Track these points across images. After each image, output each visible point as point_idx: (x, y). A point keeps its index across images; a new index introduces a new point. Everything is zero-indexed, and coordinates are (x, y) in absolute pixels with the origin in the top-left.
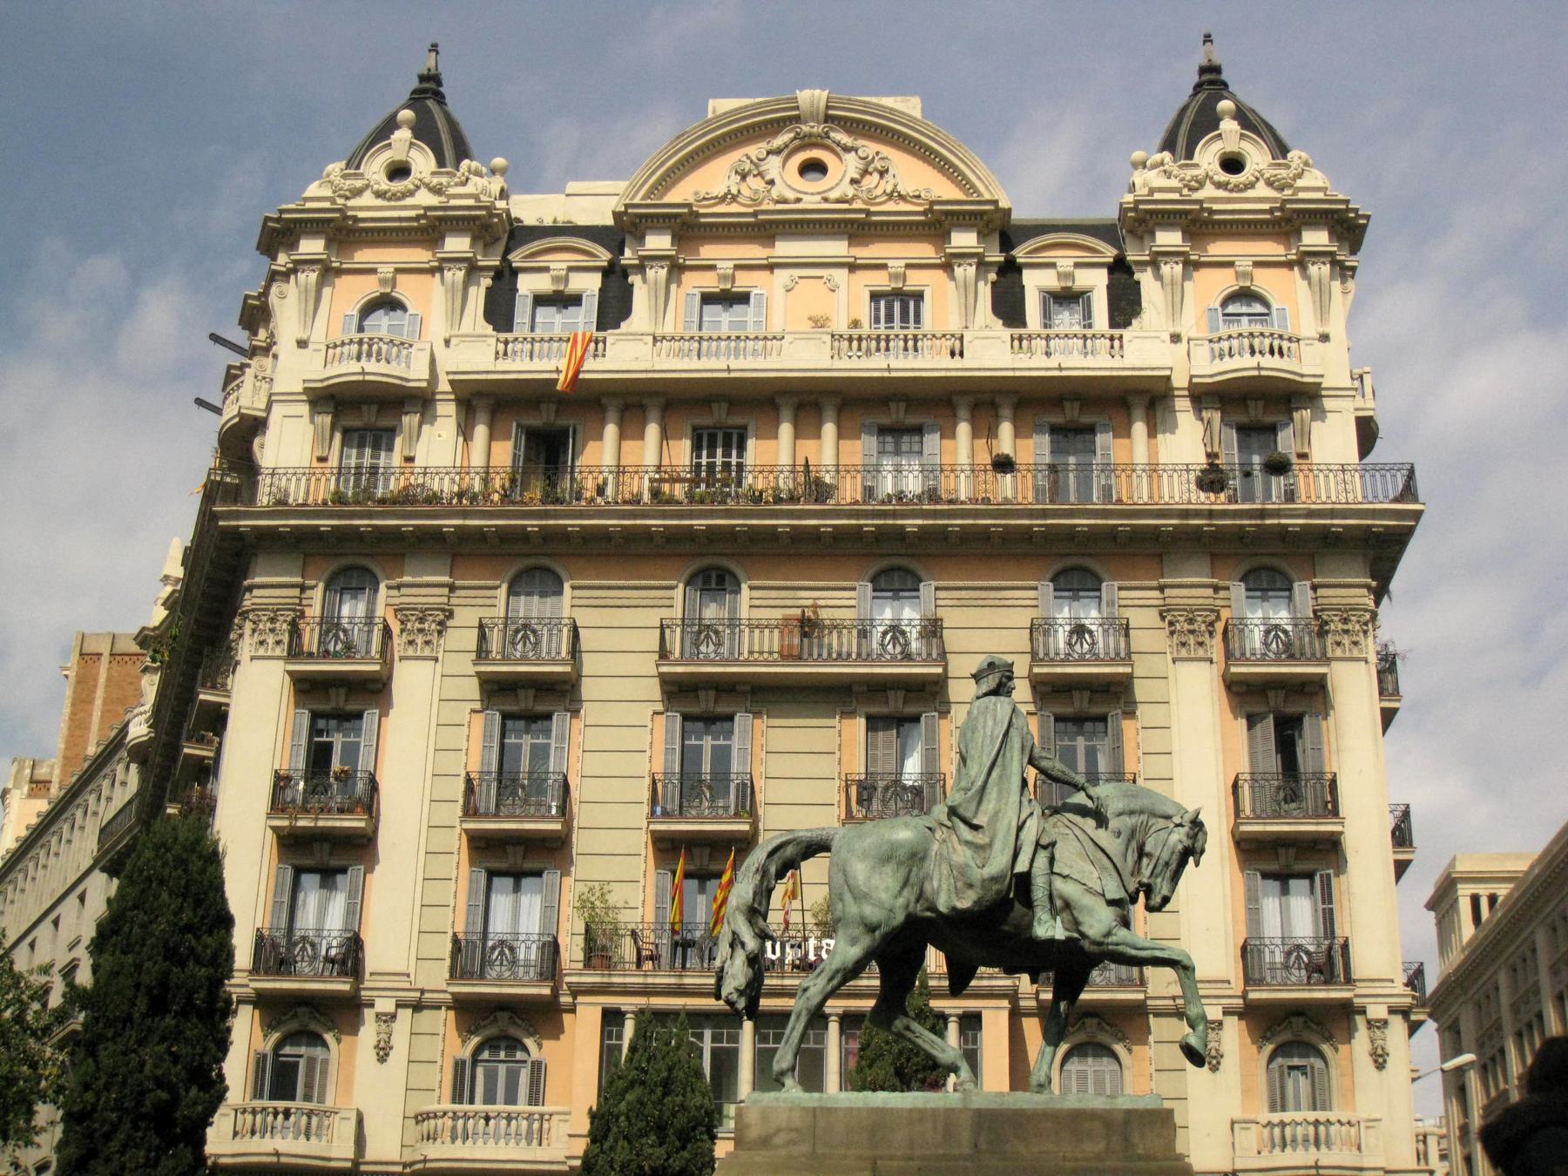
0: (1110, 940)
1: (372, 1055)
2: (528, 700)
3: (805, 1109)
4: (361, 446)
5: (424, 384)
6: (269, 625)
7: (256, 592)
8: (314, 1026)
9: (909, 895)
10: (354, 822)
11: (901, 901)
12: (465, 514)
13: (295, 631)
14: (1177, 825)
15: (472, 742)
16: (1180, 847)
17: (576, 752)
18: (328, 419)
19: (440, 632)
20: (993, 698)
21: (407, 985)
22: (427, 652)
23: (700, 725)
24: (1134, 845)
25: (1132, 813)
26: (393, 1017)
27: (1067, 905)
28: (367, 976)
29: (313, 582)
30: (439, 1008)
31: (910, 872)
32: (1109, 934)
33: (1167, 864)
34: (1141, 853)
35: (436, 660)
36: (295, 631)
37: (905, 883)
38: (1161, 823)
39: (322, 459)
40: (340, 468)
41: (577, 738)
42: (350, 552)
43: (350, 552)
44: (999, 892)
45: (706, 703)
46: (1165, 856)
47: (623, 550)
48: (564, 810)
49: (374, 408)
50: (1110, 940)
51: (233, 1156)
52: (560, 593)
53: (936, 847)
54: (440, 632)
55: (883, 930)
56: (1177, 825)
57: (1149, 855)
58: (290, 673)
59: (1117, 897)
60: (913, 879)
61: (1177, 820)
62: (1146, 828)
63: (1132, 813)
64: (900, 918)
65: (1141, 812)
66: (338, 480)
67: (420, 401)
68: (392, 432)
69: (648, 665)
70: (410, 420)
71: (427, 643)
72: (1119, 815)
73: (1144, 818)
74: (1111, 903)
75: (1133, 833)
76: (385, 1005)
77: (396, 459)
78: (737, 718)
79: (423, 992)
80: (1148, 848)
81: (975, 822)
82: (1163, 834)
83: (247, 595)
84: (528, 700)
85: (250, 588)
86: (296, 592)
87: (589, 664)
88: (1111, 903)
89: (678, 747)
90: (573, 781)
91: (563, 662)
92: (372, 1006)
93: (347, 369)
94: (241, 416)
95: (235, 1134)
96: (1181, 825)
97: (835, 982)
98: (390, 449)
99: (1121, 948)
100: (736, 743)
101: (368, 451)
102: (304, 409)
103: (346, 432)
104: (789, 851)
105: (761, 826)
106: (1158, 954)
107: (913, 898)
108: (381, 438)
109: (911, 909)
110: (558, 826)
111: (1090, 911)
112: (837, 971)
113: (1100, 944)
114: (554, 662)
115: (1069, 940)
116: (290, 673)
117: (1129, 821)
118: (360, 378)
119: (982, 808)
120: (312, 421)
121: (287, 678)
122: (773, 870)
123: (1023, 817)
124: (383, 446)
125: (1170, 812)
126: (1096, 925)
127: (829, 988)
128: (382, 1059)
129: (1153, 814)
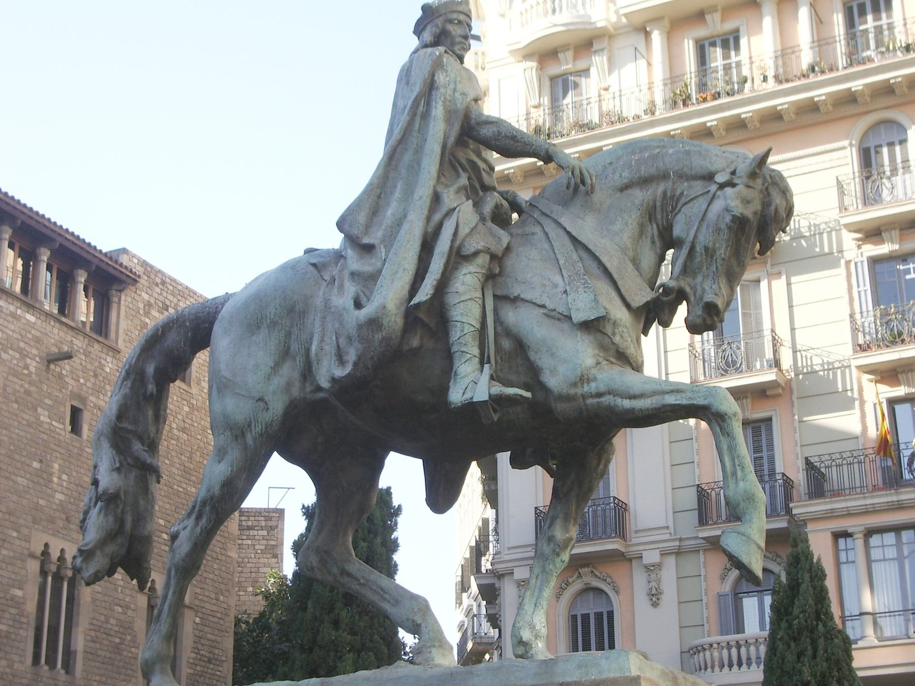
9: (290, 371)
11: (278, 381)
12: (652, 124)
14: (722, 186)
16: (728, 219)
21: (667, 537)
25: (645, 182)
26: (658, 566)
27: (521, 346)
28: (633, 535)
31: (289, 334)
34: (668, 240)
37: (285, 354)
38: (698, 187)
55: (257, 429)
56: (722, 186)
60: (294, 347)
63: (645, 182)
64: (277, 406)
72: (624, 188)
76: (651, 557)
79: (681, 540)
80: (677, 231)
81: (366, 240)
82: (702, 203)
96: (731, 184)
99: (607, 400)
107: (296, 375)
109: (296, 392)
115: (497, 401)
122: (150, 369)
123: (437, 217)
126: (562, 369)
127: (198, 530)
128: (655, 605)
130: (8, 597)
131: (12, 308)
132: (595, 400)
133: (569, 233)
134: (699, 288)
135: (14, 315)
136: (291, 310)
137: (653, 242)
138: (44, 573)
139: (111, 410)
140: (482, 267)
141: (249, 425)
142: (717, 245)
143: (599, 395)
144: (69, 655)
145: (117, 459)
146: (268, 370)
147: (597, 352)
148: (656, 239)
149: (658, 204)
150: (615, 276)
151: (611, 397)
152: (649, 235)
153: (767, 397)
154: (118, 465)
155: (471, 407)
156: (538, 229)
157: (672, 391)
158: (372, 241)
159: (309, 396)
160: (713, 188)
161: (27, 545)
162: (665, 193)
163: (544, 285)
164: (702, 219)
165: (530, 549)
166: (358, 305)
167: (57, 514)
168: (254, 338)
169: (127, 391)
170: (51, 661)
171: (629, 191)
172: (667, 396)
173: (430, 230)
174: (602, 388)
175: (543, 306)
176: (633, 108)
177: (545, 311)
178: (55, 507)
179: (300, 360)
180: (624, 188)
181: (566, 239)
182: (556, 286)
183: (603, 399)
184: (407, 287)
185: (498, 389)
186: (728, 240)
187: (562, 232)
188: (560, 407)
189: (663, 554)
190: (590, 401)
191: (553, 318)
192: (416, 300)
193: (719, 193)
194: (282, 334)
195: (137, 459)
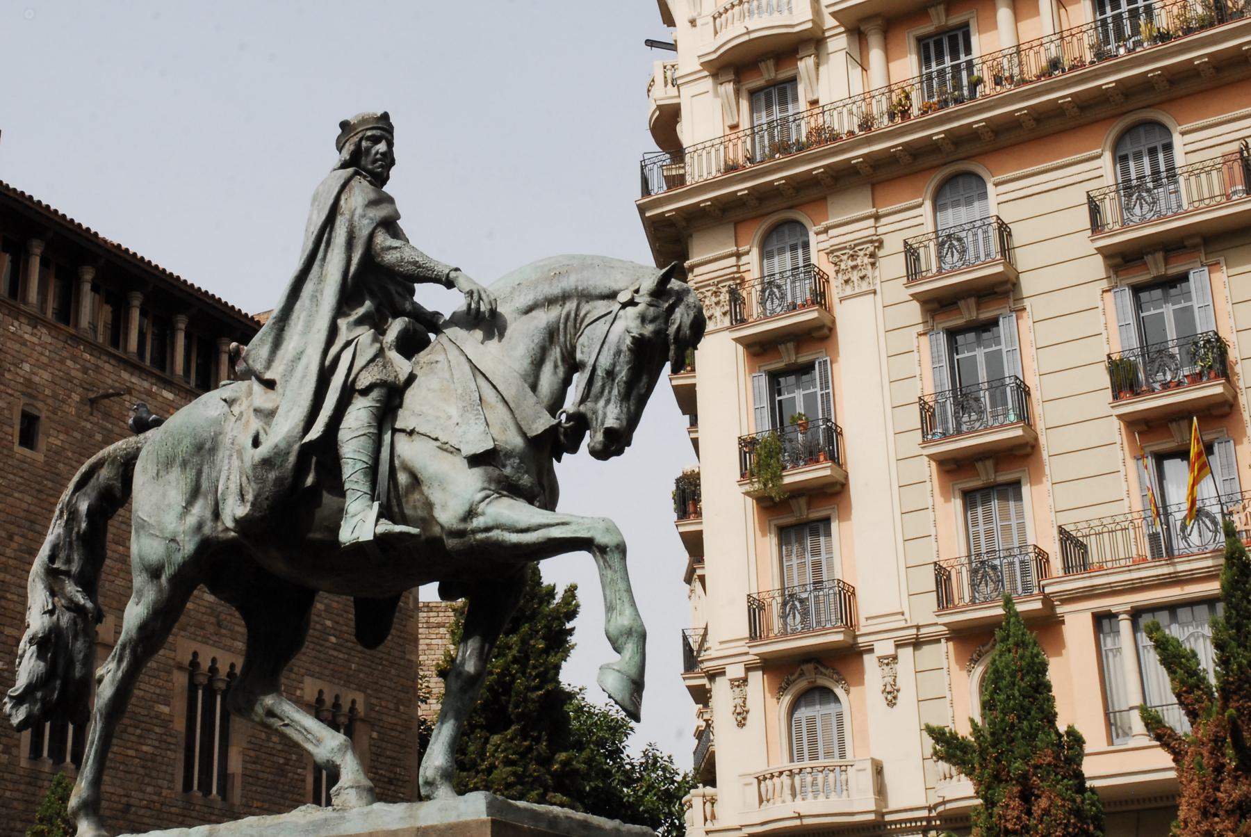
0: (477, 522)
1: (881, 700)
2: (969, 310)
4: (769, 106)
5: (809, 25)
6: (714, 299)
7: (697, 271)
8: (823, 681)
9: (200, 509)
10: (821, 471)
11: (191, 520)
12: (868, 141)
13: (735, 297)
14: (624, 306)
15: (923, 366)
16: (628, 341)
17: (1029, 352)
18: (730, 87)
19: (873, 264)
21: (903, 624)
22: (865, 286)
23: (1157, 293)
24: (556, 353)
25: (551, 301)
28: (862, 622)
29: (747, 248)
30: (938, 641)
31: (199, 473)
32: (470, 514)
33: (610, 374)
34: (573, 366)
35: (875, 292)
36: (735, 297)
37: (195, 493)
38: (601, 307)
39: (734, 127)
40: (752, 128)
41: (1027, 337)
42: (774, 208)
43: (774, 208)
44: (279, 481)
45: (1156, 268)
46: (605, 361)
47: (1037, 131)
48: (1025, 417)
49: (771, 63)
50: (477, 522)
51: (763, 824)
52: (984, 196)
54: (873, 264)
56: (624, 306)
58: (737, 340)
59: (480, 449)
60: (205, 485)
61: (624, 297)
62: (576, 324)
63: (551, 301)
64: (188, 546)
65: (564, 298)
66: (753, 140)
67: (813, 41)
68: (793, 80)
69: (1086, 244)
70: (805, 65)
71: (862, 278)
72: (529, 310)
73: (571, 306)
74: (475, 461)
75: (552, 334)
76: (885, 647)
77: (803, 105)
78: (1191, 277)
79: (918, 627)
80: (579, 356)
81: (268, 376)
83: (690, 276)
84: (969, 310)
85: (691, 269)
86: (733, 260)
87: (1023, 259)
88: (475, 461)
89: (1131, 320)
90: (1032, 381)
91: (994, 262)
92: (871, 651)
93: (736, 31)
94: (659, 107)
95: (761, 801)
96: (632, 303)
97: (124, 665)
98: (795, 99)
100: (1195, 303)
101: (776, 108)
102: (709, 83)
103: (753, 94)
104: (105, 473)
105: (1241, 384)
106: (556, 533)
108: (784, 90)
109: (207, 530)
110: (1020, 432)
111: (442, 484)
112: (124, 647)
113: (461, 534)
114: (985, 265)
115: (382, 540)
116: (737, 340)
117: (543, 318)
118: (746, 38)
119: (280, 353)
120: (716, 94)
121: (740, 348)
122: (83, 507)
124: (790, 99)
125: (615, 287)
127: (120, 674)
129: (586, 296)
130: (153, 714)
131: (146, 385)
133: (470, 361)
134: (600, 413)
135: (149, 393)
136: (199, 448)
137: (556, 367)
138: (192, 687)
140: (378, 401)
141: (163, 567)
142: (618, 368)
143: (488, 529)
144: (224, 776)
145: (50, 601)
146: (179, 509)
147: (486, 485)
148: (559, 363)
149: (562, 326)
150: (512, 405)
151: (498, 532)
152: (552, 358)
153: (1015, 457)
154: (50, 607)
155: (358, 547)
156: (441, 358)
157: (558, 524)
159: (221, 535)
160: (616, 307)
161: (172, 655)
162: (568, 315)
163: (438, 418)
164: (604, 342)
165: (743, 643)
166: (256, 443)
167: (205, 618)
169: (61, 531)
170: (205, 787)
171: (534, 313)
172: (552, 529)
173: (327, 363)
174: (490, 523)
175: (436, 439)
176: (844, 123)
177: (438, 444)
178: (203, 610)
179: (210, 497)
180: (529, 310)
181: (467, 367)
182: (450, 417)
183: (491, 534)
184: (302, 424)
185: (386, 526)
186: (628, 363)
187: (463, 359)
188: (451, 543)
189: (898, 646)
190: (480, 536)
191: (446, 450)
192: (308, 438)
193: (622, 312)
194: (194, 472)
195: (70, 600)
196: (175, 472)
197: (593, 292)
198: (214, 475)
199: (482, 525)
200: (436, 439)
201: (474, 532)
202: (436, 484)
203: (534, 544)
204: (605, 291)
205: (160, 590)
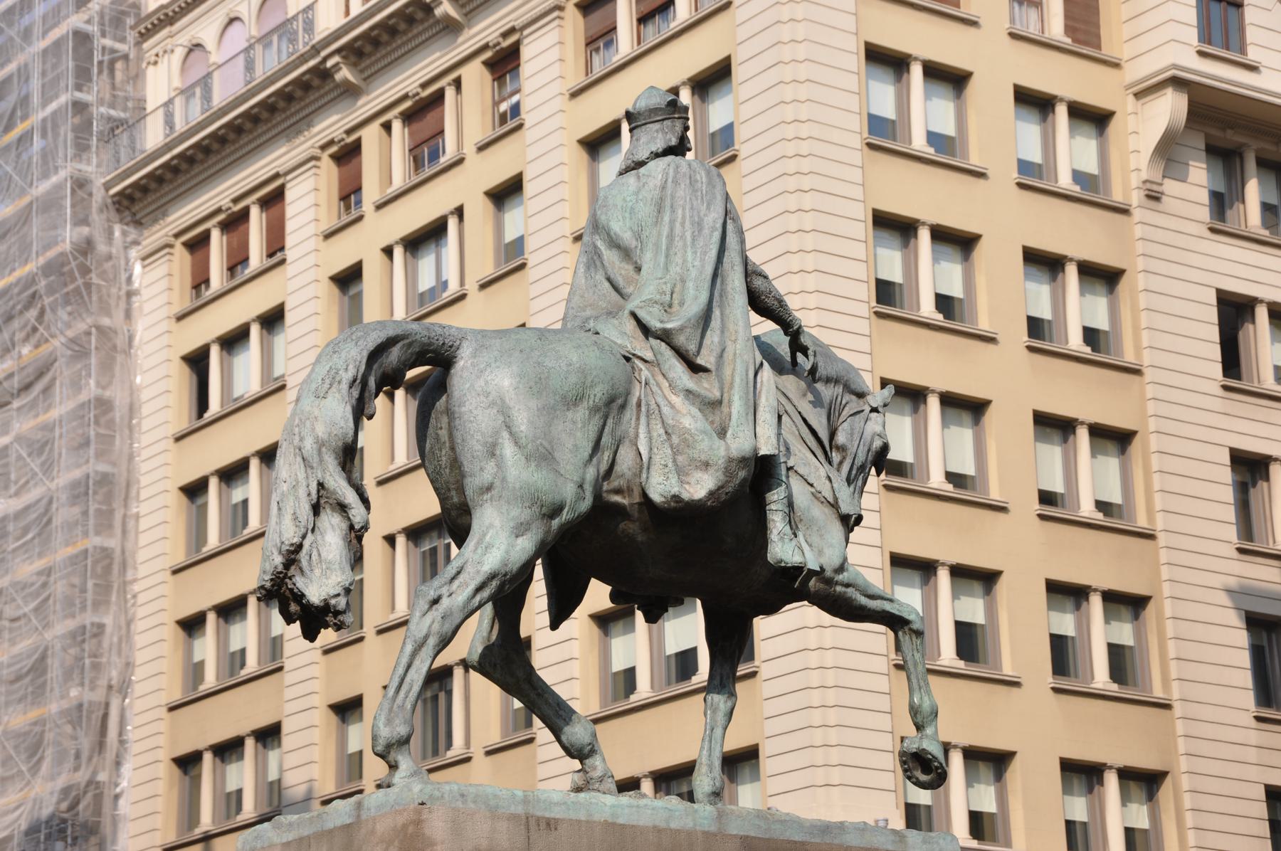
0: (840, 577)
3: (513, 817)
20: (670, 158)
53: (637, 391)
55: (565, 516)
57: (842, 449)
73: (839, 389)
112: (492, 576)
132: (843, 589)
139: (346, 421)
143: (848, 585)
158: (708, 366)
168: (570, 414)
175: (812, 485)
190: (839, 589)
191: (817, 499)
196: (581, 413)
197: (853, 387)
198: (618, 433)
199: (846, 581)
200: (812, 485)
201: (837, 583)
202: (815, 529)
203: (874, 611)
204: (859, 390)
205: (548, 532)
